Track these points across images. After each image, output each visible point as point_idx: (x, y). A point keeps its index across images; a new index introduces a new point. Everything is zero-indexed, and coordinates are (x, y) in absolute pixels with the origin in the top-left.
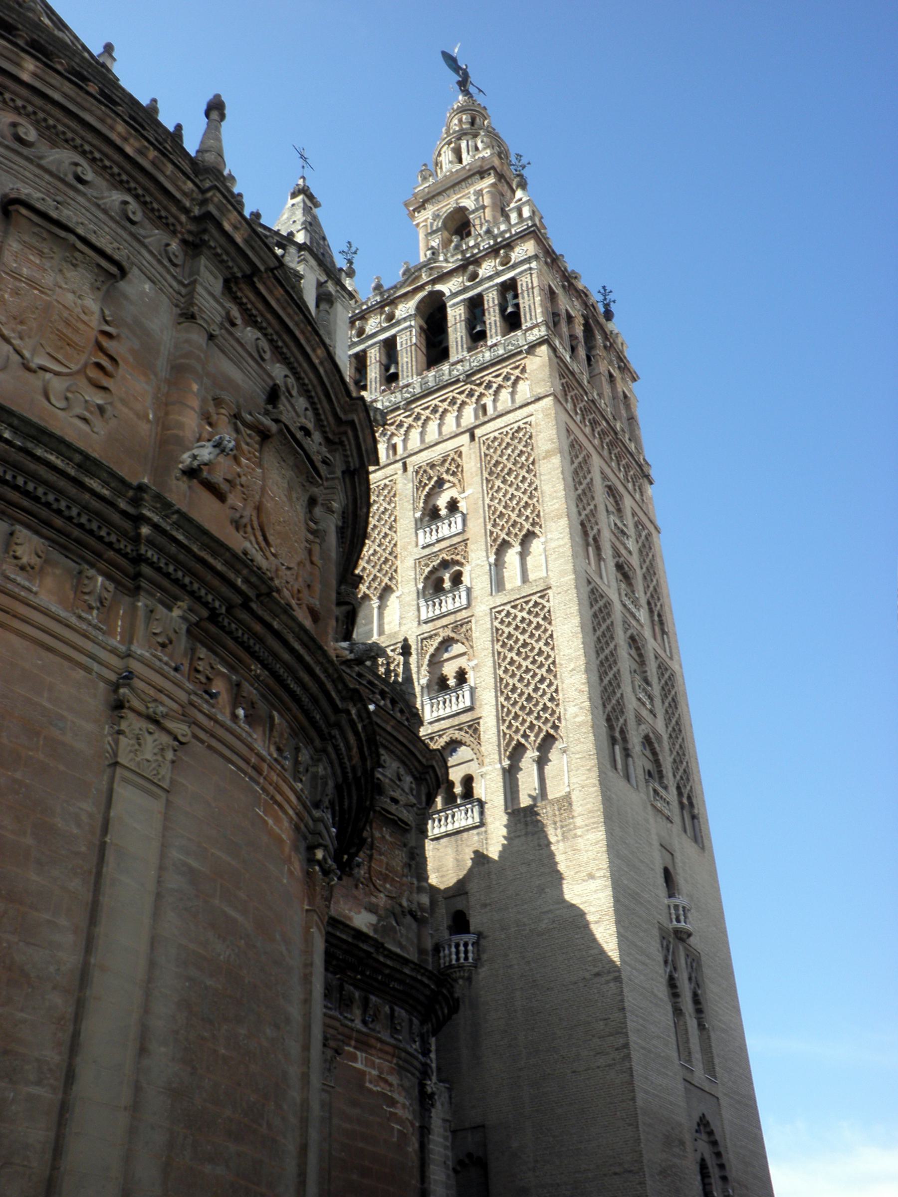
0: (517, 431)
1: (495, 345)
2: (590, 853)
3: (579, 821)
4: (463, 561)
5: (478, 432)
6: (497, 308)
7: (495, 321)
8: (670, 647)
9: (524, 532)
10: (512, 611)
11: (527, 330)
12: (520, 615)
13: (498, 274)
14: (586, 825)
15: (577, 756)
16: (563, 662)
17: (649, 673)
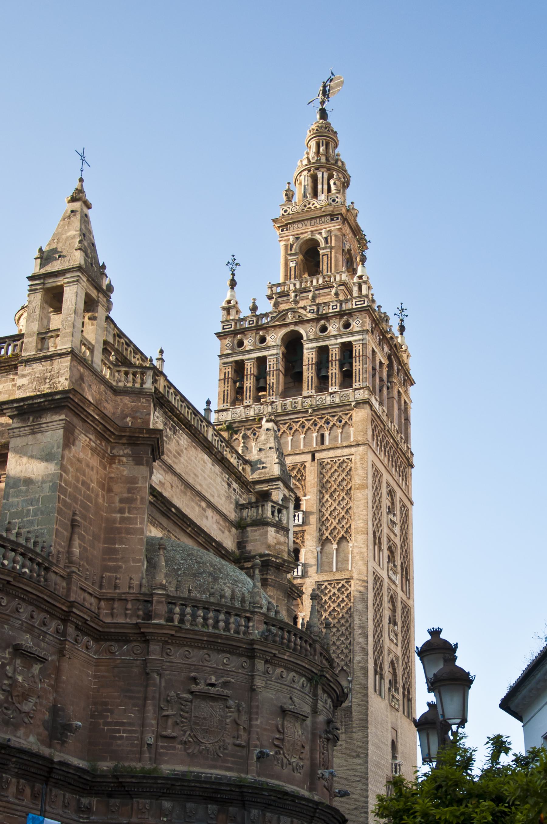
0: (342, 463)
1: (335, 393)
2: (359, 743)
3: (355, 724)
4: (301, 544)
5: (318, 456)
6: (337, 362)
7: (335, 373)
8: (409, 589)
9: (340, 536)
10: (329, 587)
11: (356, 389)
12: (333, 591)
13: (340, 335)
14: (359, 727)
15: (357, 686)
16: (355, 628)
17: (397, 617)
